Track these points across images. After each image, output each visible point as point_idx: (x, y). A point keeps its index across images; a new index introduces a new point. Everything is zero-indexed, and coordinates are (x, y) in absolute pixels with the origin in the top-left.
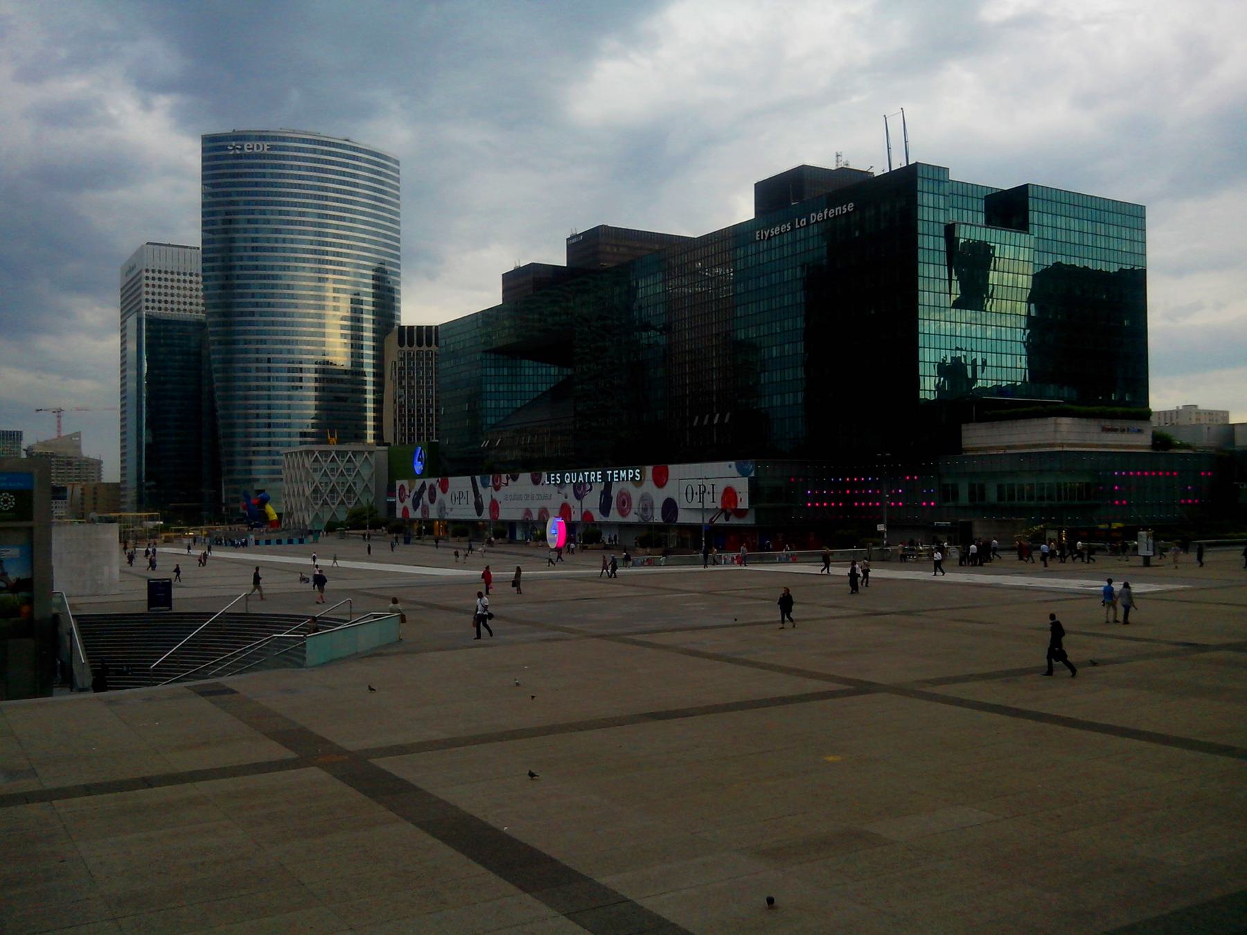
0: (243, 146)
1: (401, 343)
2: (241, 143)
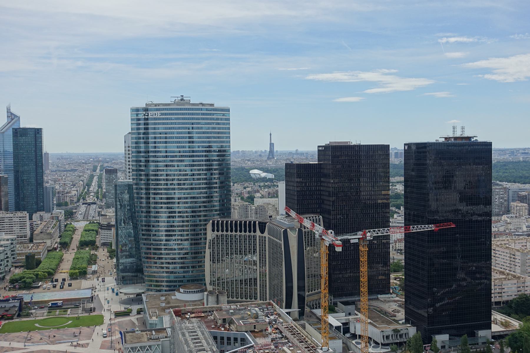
0: (148, 114)
1: (213, 231)
2: (147, 112)
